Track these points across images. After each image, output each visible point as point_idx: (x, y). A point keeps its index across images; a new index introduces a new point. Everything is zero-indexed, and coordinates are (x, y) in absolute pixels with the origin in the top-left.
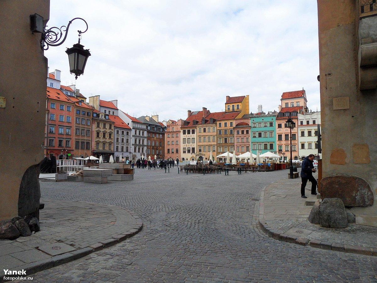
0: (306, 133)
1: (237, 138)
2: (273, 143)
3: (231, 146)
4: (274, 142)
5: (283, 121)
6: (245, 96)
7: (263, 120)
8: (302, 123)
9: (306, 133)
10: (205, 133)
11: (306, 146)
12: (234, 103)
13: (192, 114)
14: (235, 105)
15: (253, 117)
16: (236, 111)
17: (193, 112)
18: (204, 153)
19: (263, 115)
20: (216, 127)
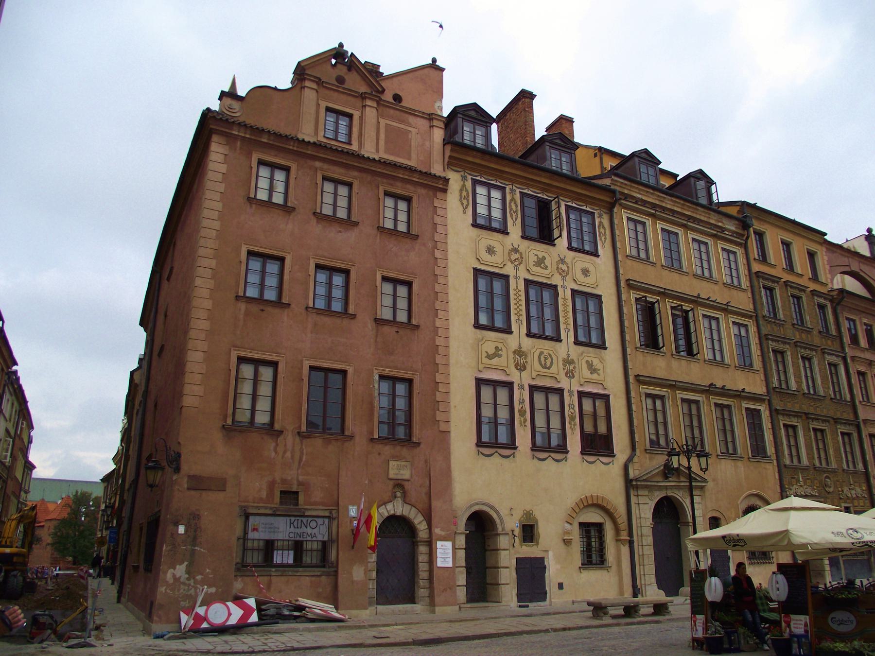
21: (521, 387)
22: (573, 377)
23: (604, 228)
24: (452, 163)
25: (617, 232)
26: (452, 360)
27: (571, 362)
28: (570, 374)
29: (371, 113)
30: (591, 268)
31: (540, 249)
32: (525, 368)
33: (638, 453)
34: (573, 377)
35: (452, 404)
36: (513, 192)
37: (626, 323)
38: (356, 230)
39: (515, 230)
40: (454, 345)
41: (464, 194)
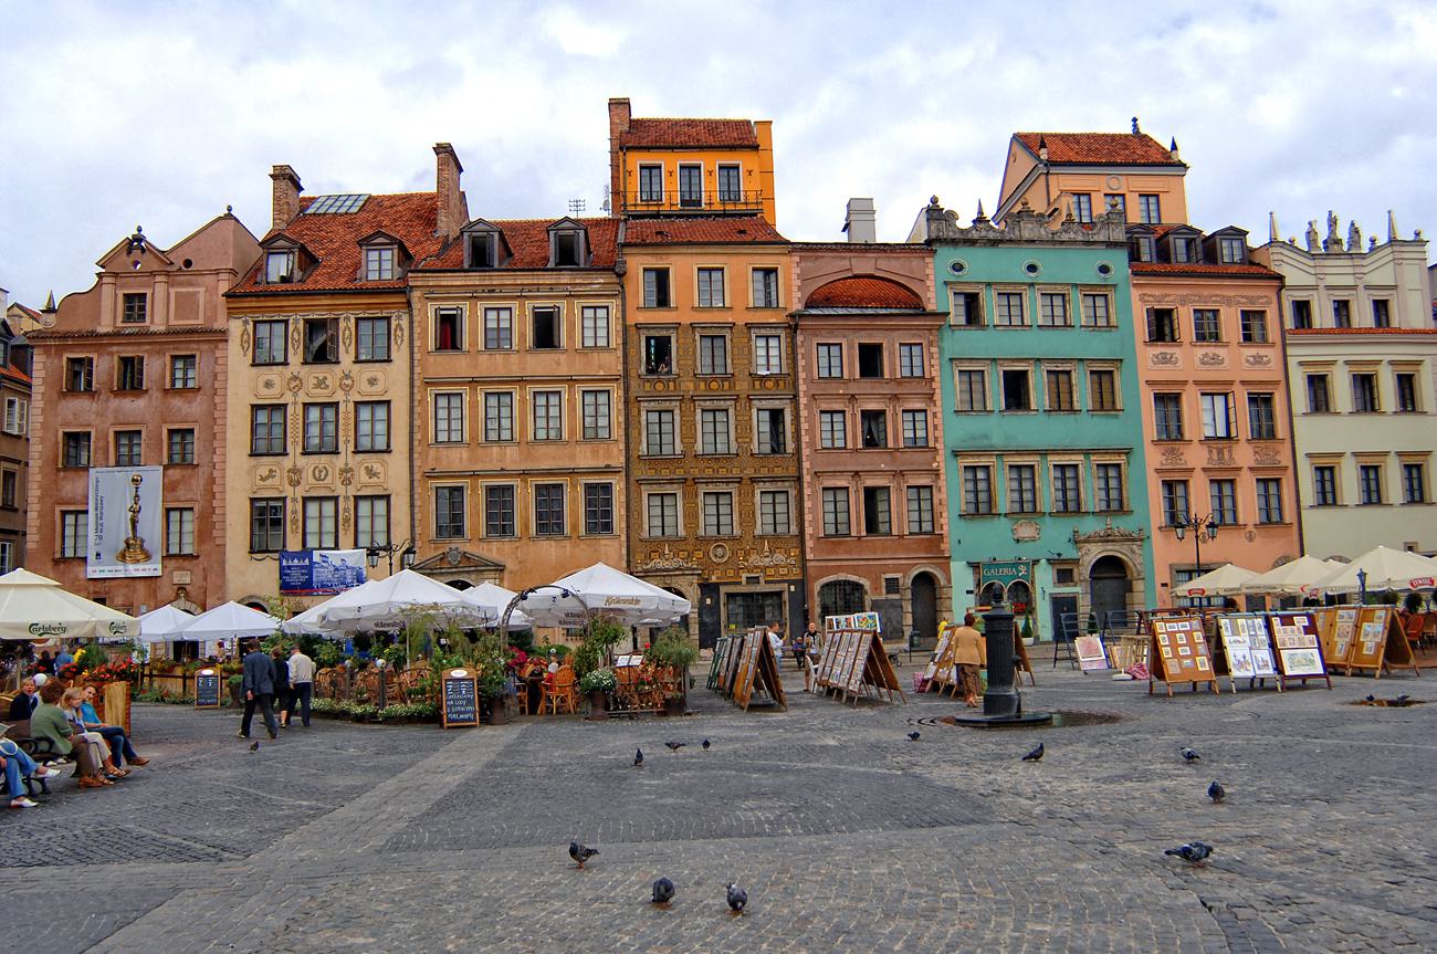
0: (1342, 390)
1: (824, 406)
2: (1121, 460)
3: (773, 480)
4: (1128, 452)
5: (1185, 292)
6: (748, 122)
7: (1032, 268)
8: (1302, 309)
9: (1342, 390)
10: (499, 358)
11: (1349, 483)
12: (701, 148)
13: (303, 209)
14: (709, 162)
15: (953, 242)
16: (725, 215)
17: (312, 200)
18: (493, 550)
19: (1028, 230)
20: (614, 304)
21: (294, 500)
22: (350, 483)
23: (402, 330)
24: (232, 312)
25: (417, 330)
26: (228, 487)
27: (351, 470)
28: (347, 482)
29: (160, 289)
30: (380, 376)
31: (320, 370)
32: (299, 483)
33: (418, 544)
34: (350, 483)
35: (228, 523)
36: (296, 321)
37: (417, 422)
38: (147, 396)
39: (295, 358)
40: (230, 473)
41: (245, 337)
